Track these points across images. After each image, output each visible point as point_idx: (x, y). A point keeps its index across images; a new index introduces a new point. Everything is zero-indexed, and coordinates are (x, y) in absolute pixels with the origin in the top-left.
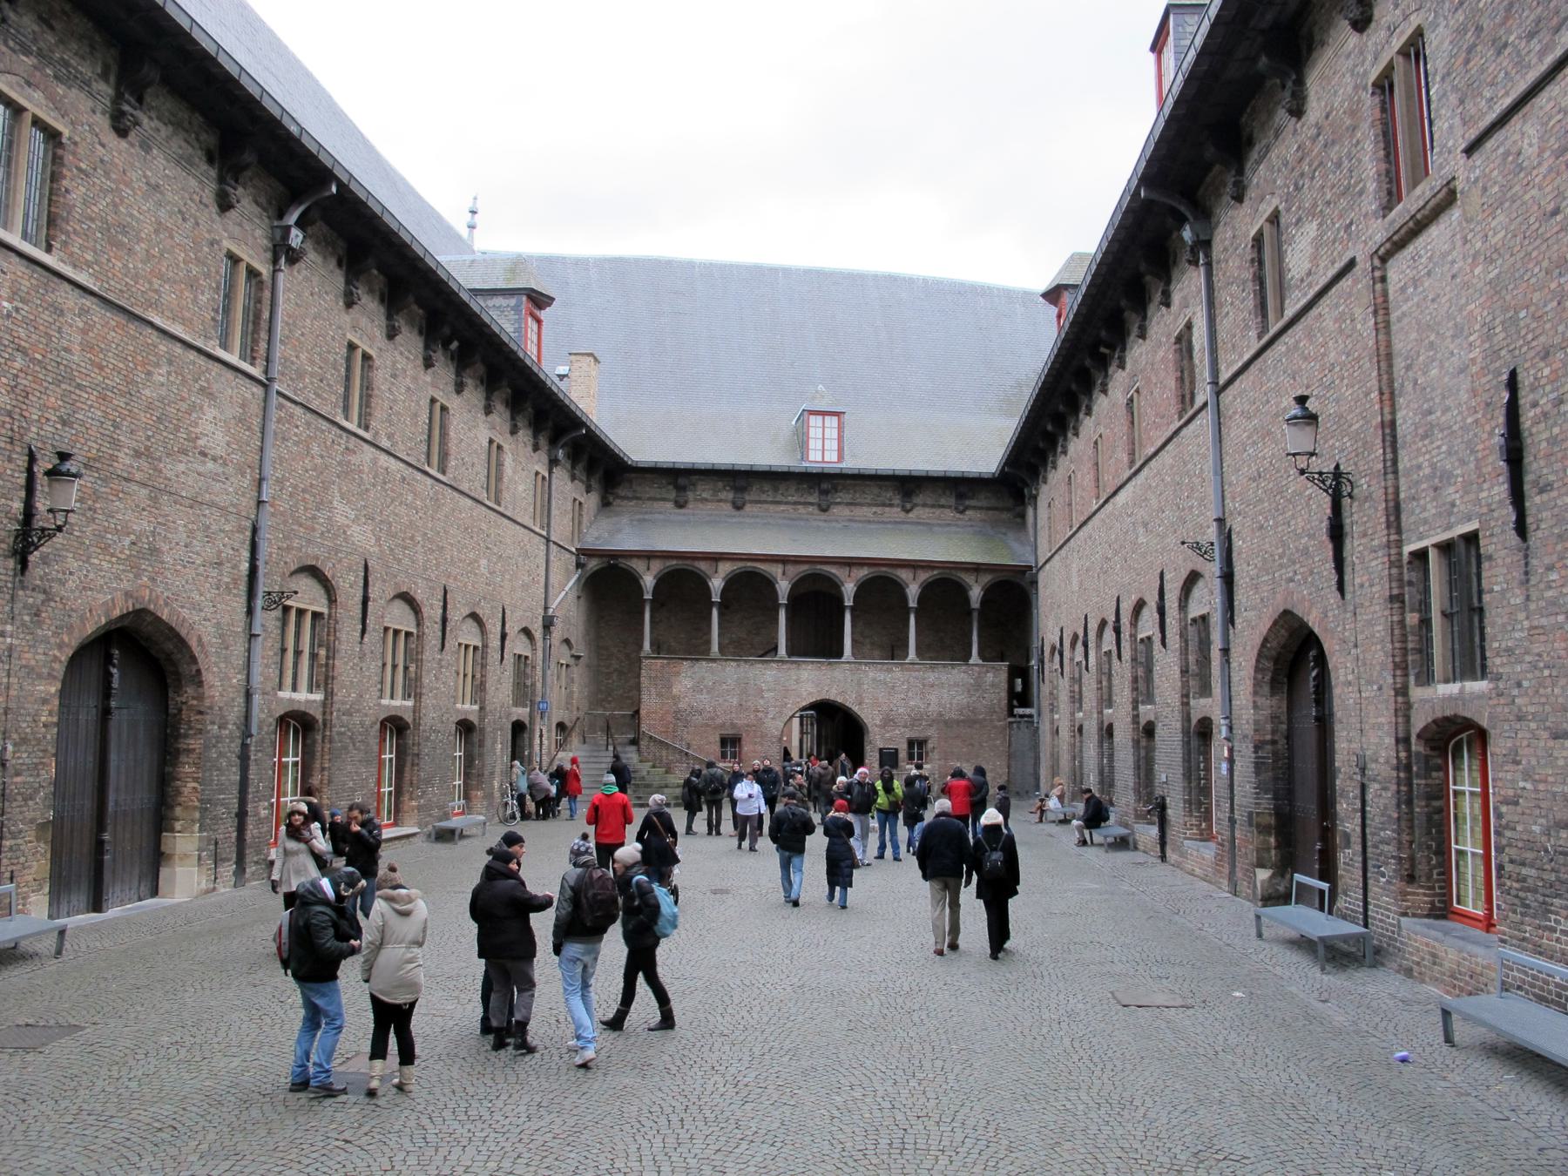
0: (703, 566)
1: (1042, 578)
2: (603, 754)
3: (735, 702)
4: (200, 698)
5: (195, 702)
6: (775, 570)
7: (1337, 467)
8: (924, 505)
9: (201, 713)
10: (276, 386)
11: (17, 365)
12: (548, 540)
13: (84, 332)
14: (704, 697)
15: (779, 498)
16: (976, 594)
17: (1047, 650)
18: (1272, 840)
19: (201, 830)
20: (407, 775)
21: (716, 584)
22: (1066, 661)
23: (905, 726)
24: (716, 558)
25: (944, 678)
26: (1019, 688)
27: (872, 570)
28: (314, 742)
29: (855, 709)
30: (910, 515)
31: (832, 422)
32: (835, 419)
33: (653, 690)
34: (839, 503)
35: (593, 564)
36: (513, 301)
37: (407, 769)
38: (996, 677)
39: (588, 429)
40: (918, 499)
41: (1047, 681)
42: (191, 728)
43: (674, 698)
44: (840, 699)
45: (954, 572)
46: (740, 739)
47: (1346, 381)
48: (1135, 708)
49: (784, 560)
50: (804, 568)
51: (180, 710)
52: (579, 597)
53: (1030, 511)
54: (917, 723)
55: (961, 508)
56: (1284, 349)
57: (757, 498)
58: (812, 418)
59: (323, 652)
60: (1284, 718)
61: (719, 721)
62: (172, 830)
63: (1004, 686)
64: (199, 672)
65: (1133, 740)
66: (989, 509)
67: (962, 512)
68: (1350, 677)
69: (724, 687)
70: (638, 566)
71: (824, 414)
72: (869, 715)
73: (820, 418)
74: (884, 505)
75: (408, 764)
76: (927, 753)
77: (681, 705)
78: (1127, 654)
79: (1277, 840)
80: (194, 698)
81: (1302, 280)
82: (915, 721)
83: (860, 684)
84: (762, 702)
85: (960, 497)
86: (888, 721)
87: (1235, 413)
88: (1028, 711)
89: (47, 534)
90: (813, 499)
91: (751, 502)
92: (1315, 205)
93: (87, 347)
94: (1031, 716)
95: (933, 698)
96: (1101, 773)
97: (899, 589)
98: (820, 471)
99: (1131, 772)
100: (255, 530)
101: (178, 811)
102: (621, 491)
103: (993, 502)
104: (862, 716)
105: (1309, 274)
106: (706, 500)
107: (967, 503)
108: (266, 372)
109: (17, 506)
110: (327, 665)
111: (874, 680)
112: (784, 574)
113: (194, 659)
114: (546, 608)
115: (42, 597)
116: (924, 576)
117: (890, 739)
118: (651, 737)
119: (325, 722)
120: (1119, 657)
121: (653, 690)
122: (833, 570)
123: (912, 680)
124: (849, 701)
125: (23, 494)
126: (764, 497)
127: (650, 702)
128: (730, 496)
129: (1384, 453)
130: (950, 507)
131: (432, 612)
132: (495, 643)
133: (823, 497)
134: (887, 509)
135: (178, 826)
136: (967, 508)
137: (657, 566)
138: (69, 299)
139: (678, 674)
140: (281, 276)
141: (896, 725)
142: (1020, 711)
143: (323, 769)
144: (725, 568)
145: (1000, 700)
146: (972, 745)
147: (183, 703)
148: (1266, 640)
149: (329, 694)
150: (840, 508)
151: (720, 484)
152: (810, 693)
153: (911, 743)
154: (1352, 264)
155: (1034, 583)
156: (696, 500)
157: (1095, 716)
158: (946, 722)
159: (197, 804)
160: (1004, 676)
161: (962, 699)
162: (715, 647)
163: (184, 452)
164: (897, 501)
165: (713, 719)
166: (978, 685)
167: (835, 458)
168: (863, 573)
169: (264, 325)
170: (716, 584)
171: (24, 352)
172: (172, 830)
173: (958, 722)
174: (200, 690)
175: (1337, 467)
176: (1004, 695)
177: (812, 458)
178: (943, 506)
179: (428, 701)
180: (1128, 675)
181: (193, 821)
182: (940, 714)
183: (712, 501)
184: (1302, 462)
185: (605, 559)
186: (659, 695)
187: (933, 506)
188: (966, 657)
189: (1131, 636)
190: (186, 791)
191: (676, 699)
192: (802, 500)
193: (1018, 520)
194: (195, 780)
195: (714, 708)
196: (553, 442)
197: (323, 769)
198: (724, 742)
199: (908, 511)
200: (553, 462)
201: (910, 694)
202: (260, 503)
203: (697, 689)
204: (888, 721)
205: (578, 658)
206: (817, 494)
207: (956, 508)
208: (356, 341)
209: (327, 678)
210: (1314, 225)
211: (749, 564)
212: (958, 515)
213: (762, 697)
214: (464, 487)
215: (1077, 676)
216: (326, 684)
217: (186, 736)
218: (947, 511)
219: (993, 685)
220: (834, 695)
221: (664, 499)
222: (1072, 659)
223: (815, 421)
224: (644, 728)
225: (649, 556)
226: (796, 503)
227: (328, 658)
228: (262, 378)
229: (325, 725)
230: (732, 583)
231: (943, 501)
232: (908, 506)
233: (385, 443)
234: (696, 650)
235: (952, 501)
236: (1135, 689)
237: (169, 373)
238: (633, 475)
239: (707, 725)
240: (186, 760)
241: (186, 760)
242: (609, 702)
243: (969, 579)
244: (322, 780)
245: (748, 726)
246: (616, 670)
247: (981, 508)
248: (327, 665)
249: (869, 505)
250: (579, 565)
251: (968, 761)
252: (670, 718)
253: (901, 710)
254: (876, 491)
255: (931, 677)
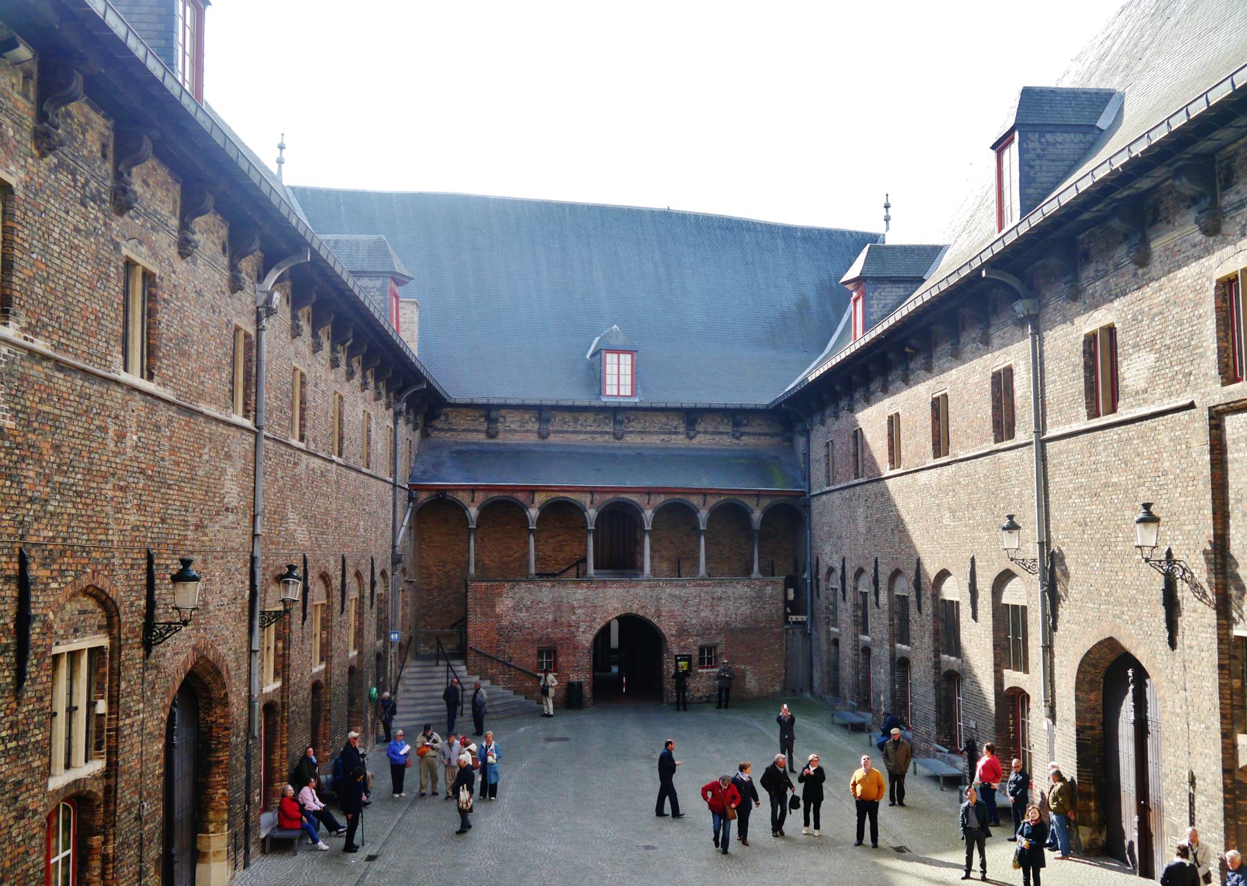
0: (520, 496)
1: (815, 504)
2: (436, 669)
3: (550, 618)
4: (226, 716)
5: (222, 721)
6: (585, 499)
7: (1169, 553)
8: (706, 432)
9: (227, 729)
10: (265, 433)
11: (141, 485)
12: (395, 485)
13: (170, 438)
14: (523, 614)
15: (579, 428)
16: (757, 516)
17: (823, 571)
18: (1092, 804)
19: (229, 828)
20: (321, 729)
21: (533, 513)
22: (849, 589)
23: (696, 636)
24: (532, 490)
25: (730, 591)
26: (791, 596)
27: (668, 497)
28: (275, 722)
29: (655, 621)
30: (694, 441)
31: (626, 359)
32: (629, 357)
33: (479, 610)
34: (631, 432)
35: (423, 497)
36: (378, 283)
37: (322, 724)
38: (774, 590)
39: (429, 383)
40: (700, 428)
41: (822, 597)
42: (219, 743)
43: (498, 616)
44: (641, 613)
45: (738, 498)
46: (555, 651)
47: (1179, 490)
48: (937, 656)
49: (592, 491)
50: (609, 497)
51: (211, 729)
52: (410, 528)
53: (800, 441)
54: (707, 632)
55: (738, 434)
56: (1116, 437)
57: (560, 428)
58: (609, 356)
59: (280, 645)
60: (1100, 709)
61: (537, 636)
62: (207, 831)
63: (781, 597)
64: (226, 695)
65: (935, 682)
66: (760, 434)
67: (738, 438)
68: (1178, 710)
69: (541, 605)
70: (463, 497)
71: (618, 352)
72: (667, 628)
73: (615, 356)
74: (670, 433)
75: (322, 720)
76: (716, 658)
77: (505, 623)
78: (928, 608)
79: (1096, 805)
80: (221, 717)
81: (1137, 393)
82: (705, 629)
83: (658, 599)
84: (574, 618)
85: (737, 424)
86: (682, 632)
87: (1061, 464)
88: (800, 618)
89: (171, 627)
90: (609, 428)
91: (554, 432)
92: (1153, 342)
93: (173, 451)
94: (803, 623)
95: (721, 610)
96: (893, 696)
97: (690, 512)
98: (617, 405)
99: (933, 708)
100: (253, 560)
101: (211, 815)
102: (438, 424)
103: (765, 429)
104: (661, 628)
105: (1145, 391)
106: (515, 431)
107: (743, 429)
108: (255, 421)
109: (143, 602)
110: (284, 655)
111: (670, 595)
112: (592, 502)
113: (224, 685)
114: (394, 547)
115: (155, 672)
116: (712, 501)
117: (685, 647)
118: (477, 652)
119: (283, 704)
120: (920, 609)
121: (479, 610)
122: (634, 498)
123: (703, 594)
124: (649, 613)
125: (145, 592)
126: (565, 428)
127: (476, 623)
128: (536, 426)
129: (1215, 558)
130: (727, 433)
131: (336, 583)
132: (368, 592)
133: (618, 427)
134: (673, 437)
135: (211, 828)
136: (743, 434)
137: (480, 497)
138: (163, 414)
139: (500, 595)
140: (264, 335)
141: (689, 635)
142: (793, 618)
143: (282, 746)
144: (540, 498)
145: (777, 610)
146: (754, 649)
147: (212, 722)
148: (1089, 652)
149: (286, 681)
150: (632, 436)
151: (527, 416)
152: (616, 609)
153: (702, 649)
154: (1191, 406)
155: (807, 506)
156: (505, 431)
157: (887, 647)
158: (732, 631)
159: (226, 807)
160: (780, 589)
161: (746, 610)
162: (533, 570)
163: (218, 513)
164: (681, 430)
165: (531, 634)
166: (759, 597)
167: (629, 393)
168: (661, 499)
169: (253, 379)
170: (533, 513)
171: (142, 472)
172: (207, 831)
173: (742, 630)
174: (227, 710)
175: (1169, 553)
176: (781, 605)
177: (608, 392)
178: (721, 433)
179: (335, 661)
180: (929, 626)
181: (223, 822)
182: (727, 623)
183: (520, 432)
184: (1147, 552)
185: (434, 493)
186: (484, 615)
187: (713, 433)
188: (748, 572)
189: (933, 595)
190: (217, 797)
191: (499, 616)
192: (599, 429)
193: (786, 444)
194: (224, 786)
195: (533, 624)
196: (397, 400)
197: (282, 746)
198: (540, 654)
199: (691, 438)
200: (397, 415)
201: (701, 607)
202: (255, 535)
203: (517, 608)
204: (682, 632)
205: (412, 582)
206: (612, 424)
207: (733, 435)
208: (297, 366)
209: (283, 668)
210: (1153, 357)
211: (562, 495)
212: (734, 441)
213: (574, 613)
214: (351, 463)
215: (860, 602)
216: (284, 672)
217: (216, 750)
218: (725, 437)
219: (771, 597)
220: (635, 608)
221: (480, 431)
222: (855, 588)
223: (611, 359)
224: (471, 644)
225: (473, 490)
226: (593, 432)
227: (284, 648)
228: (254, 428)
229: (283, 707)
230: (546, 509)
231: (722, 429)
232: (692, 433)
233: (312, 447)
234: (514, 573)
235: (729, 429)
236: (936, 640)
237: (210, 450)
238: (449, 409)
239: (527, 640)
240: (216, 770)
241: (216, 770)
242: (431, 616)
243: (750, 503)
244: (281, 756)
245: (562, 639)
246: (436, 587)
247: (754, 434)
248: (284, 655)
249: (658, 433)
250: (411, 499)
251: (750, 664)
252: (494, 635)
253: (694, 621)
254: (664, 420)
255: (719, 591)
